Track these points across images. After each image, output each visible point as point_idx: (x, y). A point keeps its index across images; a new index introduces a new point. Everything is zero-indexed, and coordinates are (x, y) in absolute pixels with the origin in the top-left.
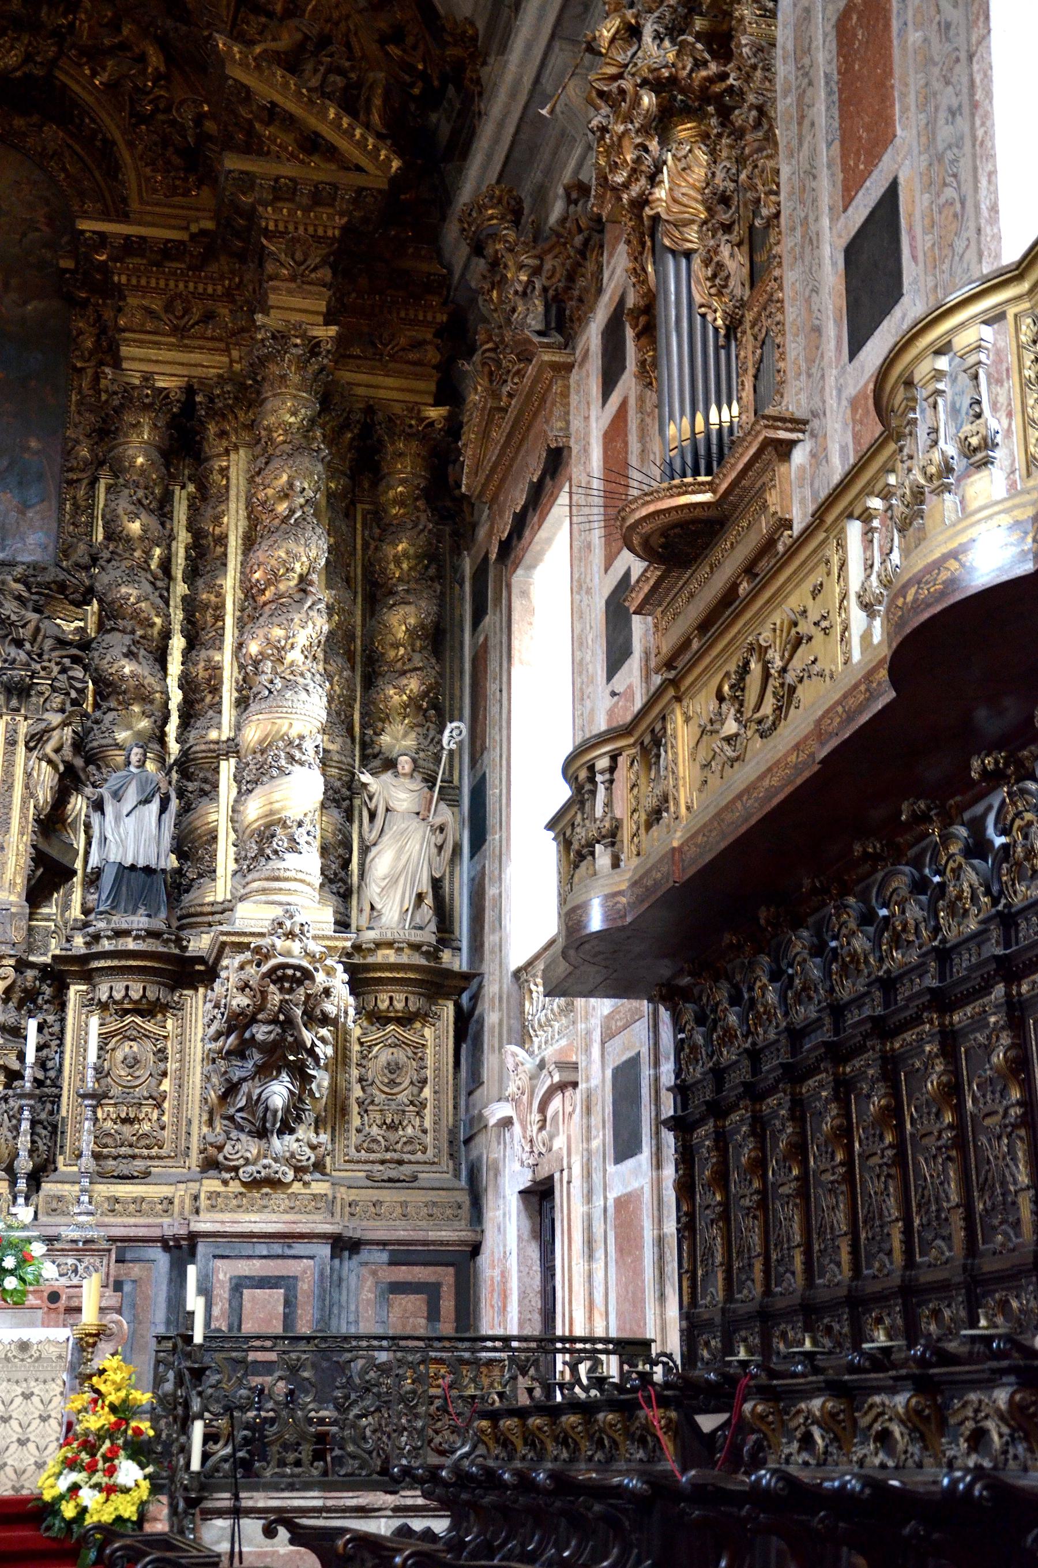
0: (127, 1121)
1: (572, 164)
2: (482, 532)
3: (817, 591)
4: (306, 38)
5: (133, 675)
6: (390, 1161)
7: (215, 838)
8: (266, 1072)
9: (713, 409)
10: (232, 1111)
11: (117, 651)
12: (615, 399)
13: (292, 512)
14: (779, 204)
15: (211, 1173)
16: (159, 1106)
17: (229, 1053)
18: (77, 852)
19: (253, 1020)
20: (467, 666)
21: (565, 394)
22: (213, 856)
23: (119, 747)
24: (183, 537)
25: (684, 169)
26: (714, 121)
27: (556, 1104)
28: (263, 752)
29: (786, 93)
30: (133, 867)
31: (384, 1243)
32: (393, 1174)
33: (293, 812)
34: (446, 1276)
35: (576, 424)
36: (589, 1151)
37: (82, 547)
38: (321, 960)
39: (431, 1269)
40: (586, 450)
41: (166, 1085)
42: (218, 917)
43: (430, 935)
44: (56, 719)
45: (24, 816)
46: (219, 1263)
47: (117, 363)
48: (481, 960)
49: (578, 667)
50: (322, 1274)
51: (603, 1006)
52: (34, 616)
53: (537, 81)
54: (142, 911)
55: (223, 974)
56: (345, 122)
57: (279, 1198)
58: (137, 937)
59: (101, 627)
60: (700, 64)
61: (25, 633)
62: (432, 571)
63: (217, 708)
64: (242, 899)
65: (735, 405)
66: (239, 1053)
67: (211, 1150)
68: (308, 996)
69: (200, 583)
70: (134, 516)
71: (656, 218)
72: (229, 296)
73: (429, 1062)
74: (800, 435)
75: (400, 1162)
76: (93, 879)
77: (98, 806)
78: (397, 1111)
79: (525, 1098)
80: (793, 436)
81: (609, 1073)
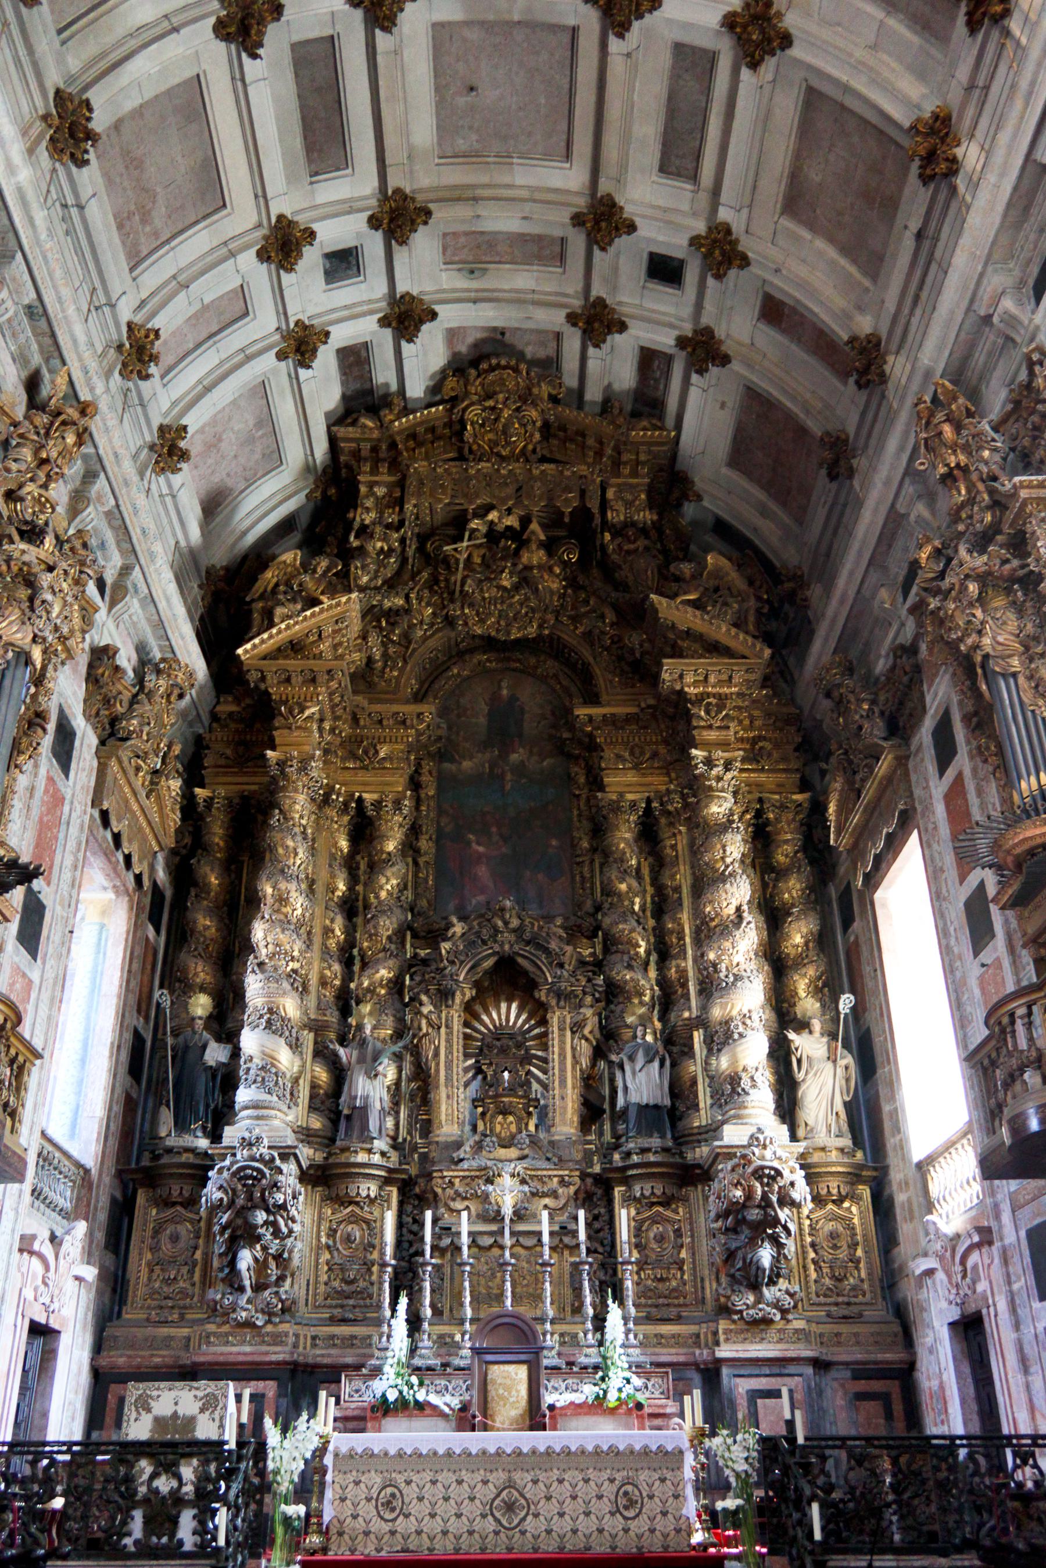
0: (661, 1280)
1: (891, 635)
2: (842, 870)
4: (706, 589)
5: (632, 979)
6: (843, 1303)
7: (694, 1082)
8: (753, 1243)
10: (732, 1271)
11: (619, 966)
12: (951, 773)
13: (727, 867)
15: (725, 1315)
16: (681, 1269)
17: (727, 1229)
18: (604, 1097)
19: (744, 1206)
20: (842, 957)
21: (907, 774)
22: (696, 1096)
23: (628, 1026)
24: (650, 890)
26: (1019, 594)
27: (974, 1258)
28: (727, 1023)
30: (647, 1105)
31: (846, 1364)
32: (846, 1312)
34: (893, 1387)
35: (917, 792)
36: (1011, 1292)
38: (786, 1162)
39: (882, 1382)
40: (928, 808)
41: (683, 1254)
42: (704, 1136)
43: (846, 1142)
44: (588, 1012)
45: (574, 1077)
46: (738, 1380)
47: (601, 788)
48: (885, 1156)
49: (946, 950)
50: (809, 1387)
51: (1014, 1185)
52: (569, 949)
53: (859, 592)
54: (656, 1135)
55: (721, 1175)
56: (733, 631)
57: (772, 1333)
58: (656, 1152)
59: (606, 950)
60: (1006, 561)
62: (813, 897)
63: (687, 996)
64: (723, 1123)
66: (734, 1230)
67: (722, 1300)
68: (780, 1188)
69: (666, 918)
70: (622, 880)
71: (986, 657)
72: (666, 742)
73: (858, 1230)
75: (848, 1304)
78: (841, 1267)
79: (948, 1254)
81: (1023, 1234)
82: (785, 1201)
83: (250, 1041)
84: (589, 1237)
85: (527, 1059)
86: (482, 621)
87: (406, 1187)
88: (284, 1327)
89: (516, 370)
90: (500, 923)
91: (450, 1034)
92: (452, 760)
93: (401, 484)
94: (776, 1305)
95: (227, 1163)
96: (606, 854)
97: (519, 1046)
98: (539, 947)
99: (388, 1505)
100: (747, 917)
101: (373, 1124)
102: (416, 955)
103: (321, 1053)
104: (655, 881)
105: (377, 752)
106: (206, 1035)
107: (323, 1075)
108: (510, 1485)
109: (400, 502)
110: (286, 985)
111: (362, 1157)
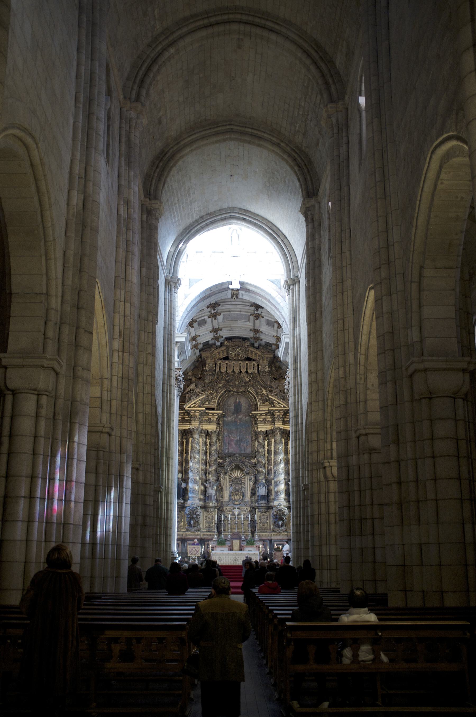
24: (266, 448)
33: (280, 490)
37: (254, 451)
41: (268, 521)
44: (252, 477)
61: (248, 466)
72: (271, 418)
76: (258, 496)
77: (258, 487)
82: (283, 515)
83: (190, 485)
84: (251, 518)
85: (241, 484)
86: (232, 388)
87: (219, 509)
88: (199, 533)
89: (239, 341)
90: (236, 459)
91: (226, 481)
92: (227, 418)
93: (216, 364)
94: (282, 530)
95: (189, 507)
96: (258, 442)
97: (239, 481)
98: (243, 464)
99: (220, 560)
100: (282, 461)
101: (213, 498)
102: (219, 462)
103: (202, 484)
104: (268, 446)
105: (211, 420)
106: (181, 482)
107: (202, 488)
108: (235, 558)
109: (216, 367)
110: (197, 475)
111: (211, 504)
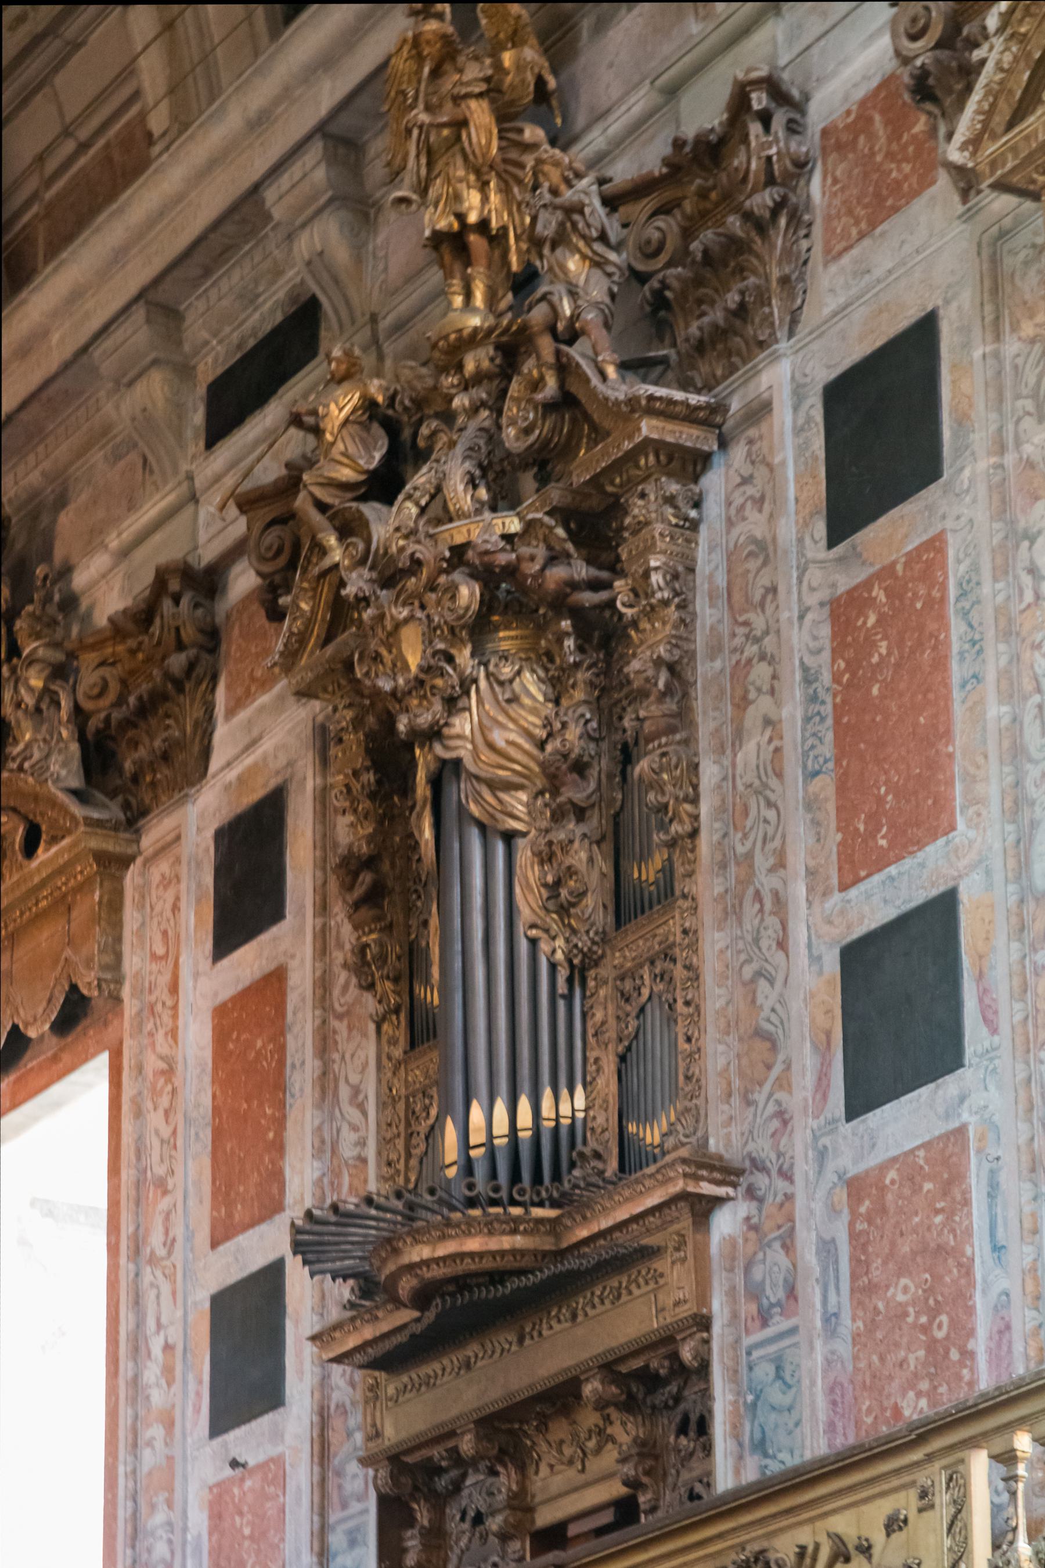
3: (894, 1524)
9: (547, 1094)
14: (696, 818)
25: (509, 701)
29: (715, 650)
65: (579, 1092)
74: (730, 1191)
80: (722, 1191)
